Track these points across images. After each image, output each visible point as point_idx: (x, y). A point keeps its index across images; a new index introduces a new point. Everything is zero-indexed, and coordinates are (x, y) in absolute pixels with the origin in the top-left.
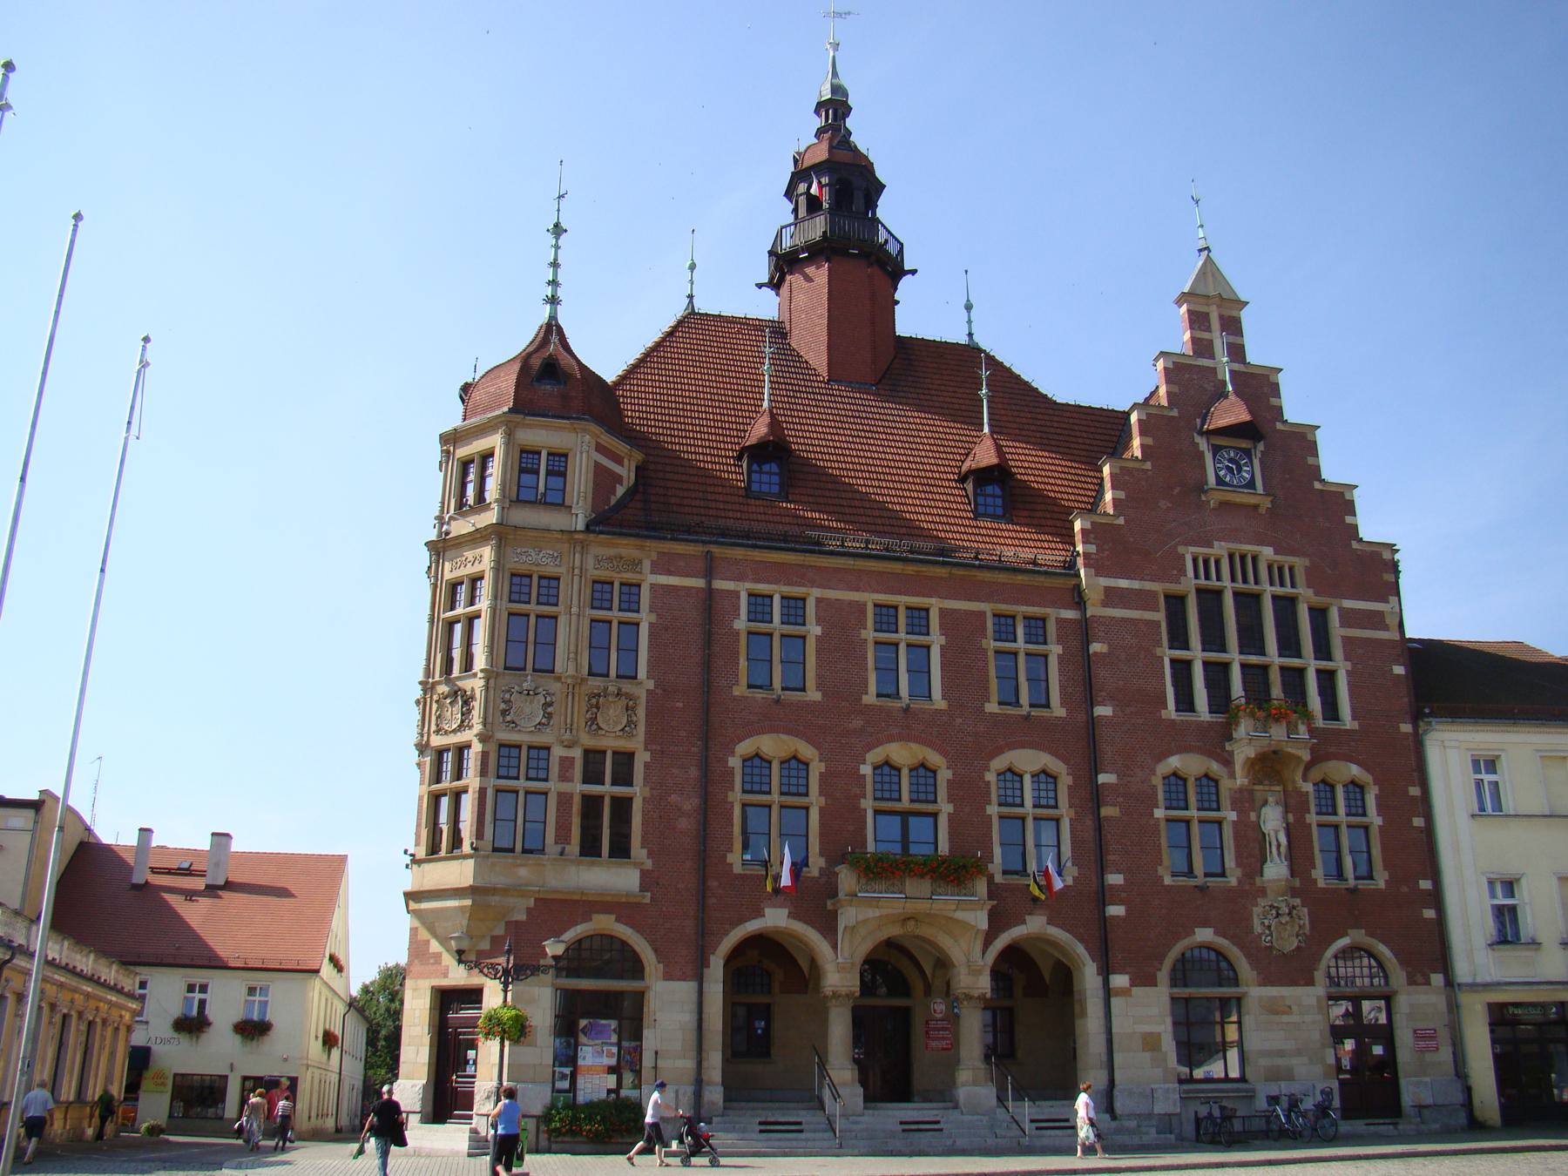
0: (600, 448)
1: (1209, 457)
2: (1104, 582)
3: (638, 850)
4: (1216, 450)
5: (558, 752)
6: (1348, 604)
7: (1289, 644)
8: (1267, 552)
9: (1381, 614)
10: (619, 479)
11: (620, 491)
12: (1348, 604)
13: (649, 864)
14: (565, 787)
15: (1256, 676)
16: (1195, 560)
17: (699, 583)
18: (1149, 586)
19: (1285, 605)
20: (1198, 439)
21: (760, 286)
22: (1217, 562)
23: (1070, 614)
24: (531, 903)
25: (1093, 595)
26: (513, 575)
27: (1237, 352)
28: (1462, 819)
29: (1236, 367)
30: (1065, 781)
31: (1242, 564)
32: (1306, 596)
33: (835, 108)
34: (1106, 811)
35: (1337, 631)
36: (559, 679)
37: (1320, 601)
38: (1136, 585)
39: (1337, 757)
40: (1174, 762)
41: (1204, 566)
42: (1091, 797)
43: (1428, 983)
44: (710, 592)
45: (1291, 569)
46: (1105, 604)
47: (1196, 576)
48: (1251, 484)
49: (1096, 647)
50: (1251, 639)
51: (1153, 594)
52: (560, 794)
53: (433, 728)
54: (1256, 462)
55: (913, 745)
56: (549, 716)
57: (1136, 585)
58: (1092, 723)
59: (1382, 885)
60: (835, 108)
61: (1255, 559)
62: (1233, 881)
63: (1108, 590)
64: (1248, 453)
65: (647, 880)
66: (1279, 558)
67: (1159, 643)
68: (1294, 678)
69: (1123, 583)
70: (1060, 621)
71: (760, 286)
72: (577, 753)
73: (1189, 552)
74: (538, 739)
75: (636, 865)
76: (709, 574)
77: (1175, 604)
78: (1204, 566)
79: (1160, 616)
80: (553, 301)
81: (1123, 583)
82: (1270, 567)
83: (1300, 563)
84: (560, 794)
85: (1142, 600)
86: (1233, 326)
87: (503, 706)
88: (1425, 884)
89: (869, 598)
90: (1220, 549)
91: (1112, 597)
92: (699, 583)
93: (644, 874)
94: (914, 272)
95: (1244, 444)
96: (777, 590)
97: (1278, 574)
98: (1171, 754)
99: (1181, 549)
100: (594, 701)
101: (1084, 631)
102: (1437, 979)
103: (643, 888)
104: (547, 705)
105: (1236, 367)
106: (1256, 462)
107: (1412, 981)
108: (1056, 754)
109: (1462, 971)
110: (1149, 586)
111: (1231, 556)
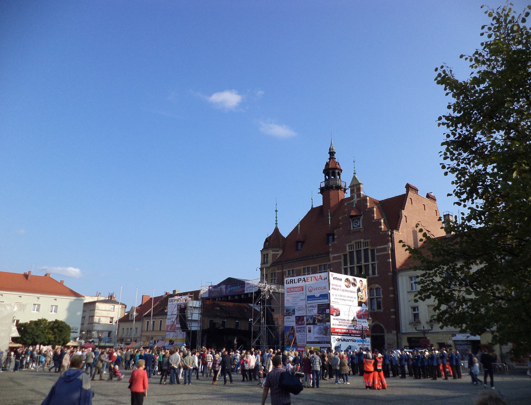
0: (273, 251)
2: (333, 256)
4: (353, 221)
6: (378, 247)
7: (366, 260)
8: (362, 240)
9: (386, 248)
10: (278, 254)
11: (278, 256)
12: (378, 247)
17: (281, 271)
18: (340, 254)
19: (366, 251)
25: (331, 259)
27: (359, 195)
28: (405, 292)
29: (359, 199)
31: (359, 244)
32: (369, 247)
33: (332, 153)
35: (376, 254)
37: (373, 248)
38: (338, 255)
39: (374, 283)
41: (351, 247)
43: (391, 332)
44: (283, 272)
48: (359, 226)
50: (359, 260)
51: (341, 256)
57: (338, 255)
59: (382, 311)
60: (332, 153)
63: (334, 257)
64: (359, 219)
67: (341, 266)
68: (367, 267)
69: (336, 255)
76: (282, 269)
77: (345, 256)
79: (342, 260)
80: (276, 224)
81: (336, 255)
83: (368, 240)
85: (339, 257)
86: (359, 189)
88: (392, 310)
89: (302, 268)
90: (353, 242)
91: (334, 258)
92: (281, 271)
96: (291, 269)
97: (366, 244)
102: (394, 332)
105: (359, 199)
106: (361, 220)
107: (388, 332)
109: (404, 329)
110: (340, 254)
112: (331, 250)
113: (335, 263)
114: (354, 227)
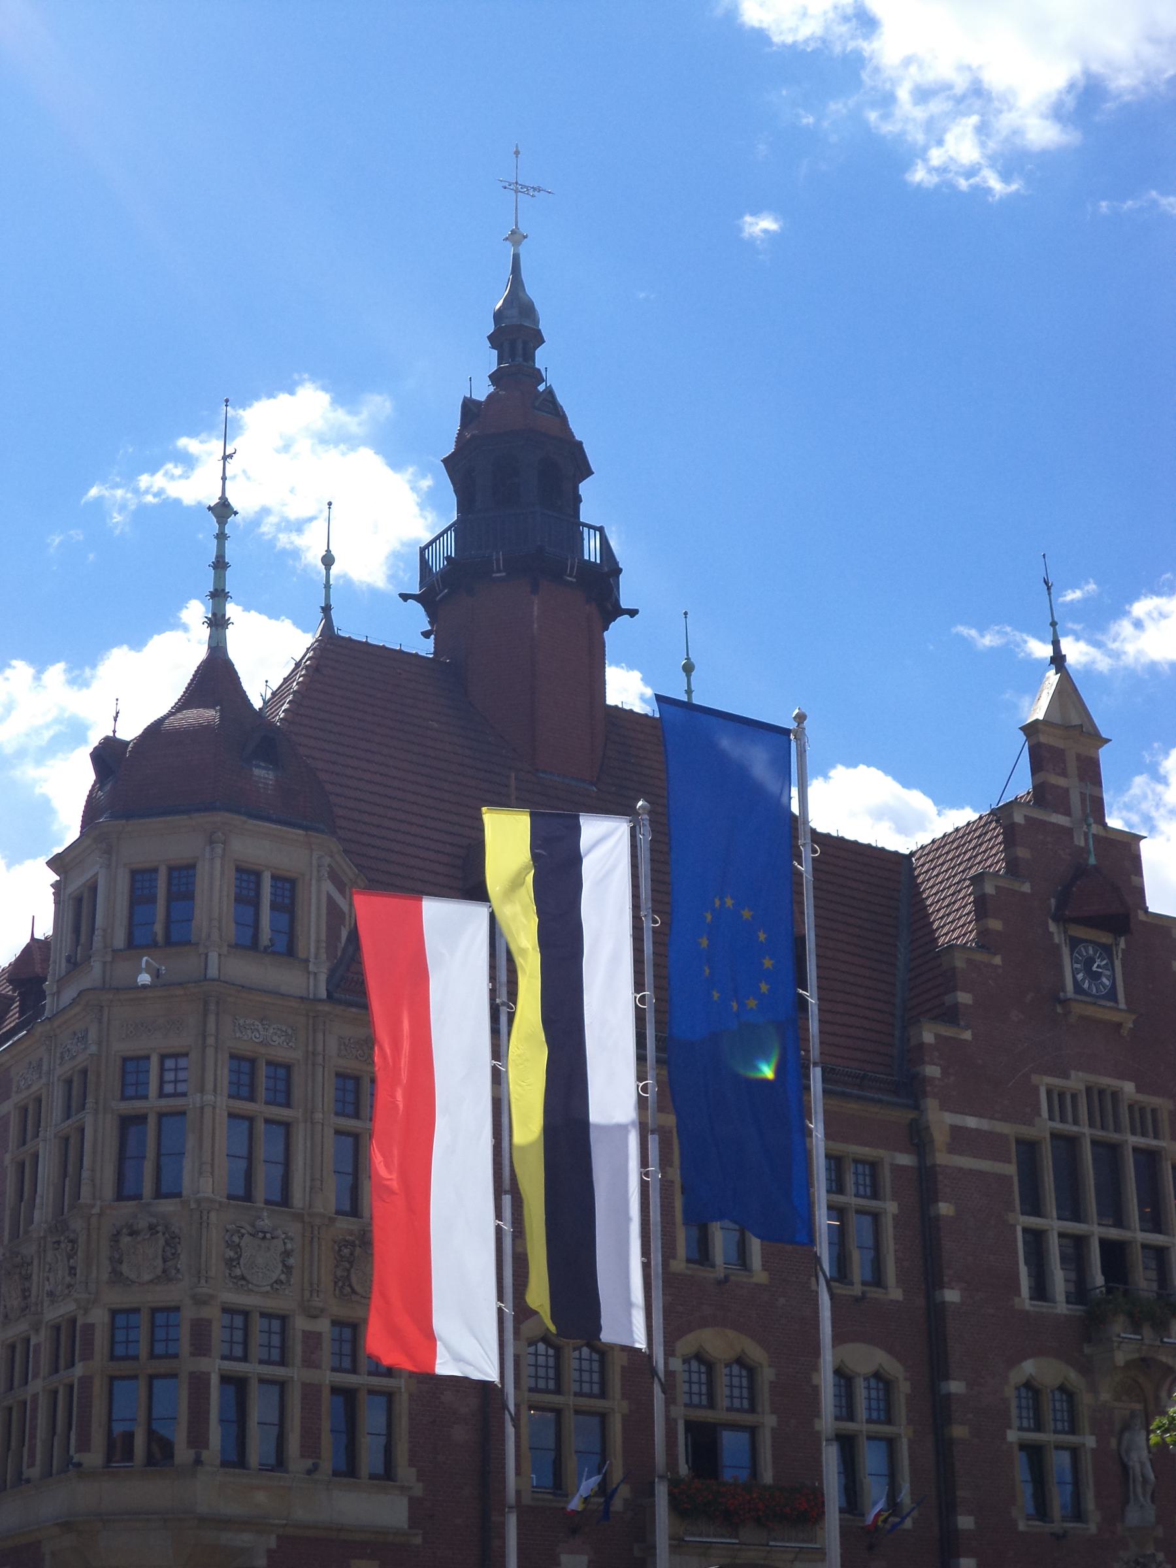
1: (1066, 951)
2: (950, 1118)
3: (405, 1472)
4: (1074, 943)
5: (301, 1323)
8: (1129, 1087)
13: (418, 1490)
14: (310, 1375)
15: (1114, 1253)
16: (1049, 1093)
20: (1052, 927)
21: (405, 597)
22: (1074, 1097)
23: (905, 1159)
24: (272, 1543)
25: (940, 1137)
26: (233, 1057)
30: (904, 1388)
31: (1102, 1102)
34: (959, 1431)
36: (299, 1217)
40: (1029, 1367)
41: (1060, 1102)
42: (937, 1412)
45: (1154, 1111)
46: (952, 1150)
47: (1051, 1118)
48: (1112, 995)
49: (945, 1208)
52: (305, 1385)
53: (105, 1276)
54: (1118, 964)
55: (731, 1334)
56: (288, 1269)
58: (936, 1313)
61: (1115, 1095)
62: (1093, 1528)
63: (956, 1130)
64: (1107, 951)
65: (419, 1513)
66: (1140, 1097)
69: (971, 1122)
70: (897, 1169)
71: (405, 597)
72: (323, 1326)
73: (1044, 1082)
74: (270, 1304)
75: (403, 1489)
77: (1028, 1150)
78: (1060, 1102)
79: (1011, 1169)
81: (971, 1122)
82: (1131, 1107)
84: (305, 1385)
87: (231, 1254)
90: (1076, 1081)
91: (960, 1139)
93: (414, 1503)
94: (633, 613)
95: (1105, 938)
97: (1143, 1120)
98: (1025, 1358)
99: (1035, 1079)
100: (346, 1251)
101: (925, 1183)
103: (414, 1521)
104: (287, 1254)
106: (1118, 964)
108: (890, 1351)
111: (1089, 1090)
112: (932, 1071)
113: (980, 1174)
114: (1077, 986)
